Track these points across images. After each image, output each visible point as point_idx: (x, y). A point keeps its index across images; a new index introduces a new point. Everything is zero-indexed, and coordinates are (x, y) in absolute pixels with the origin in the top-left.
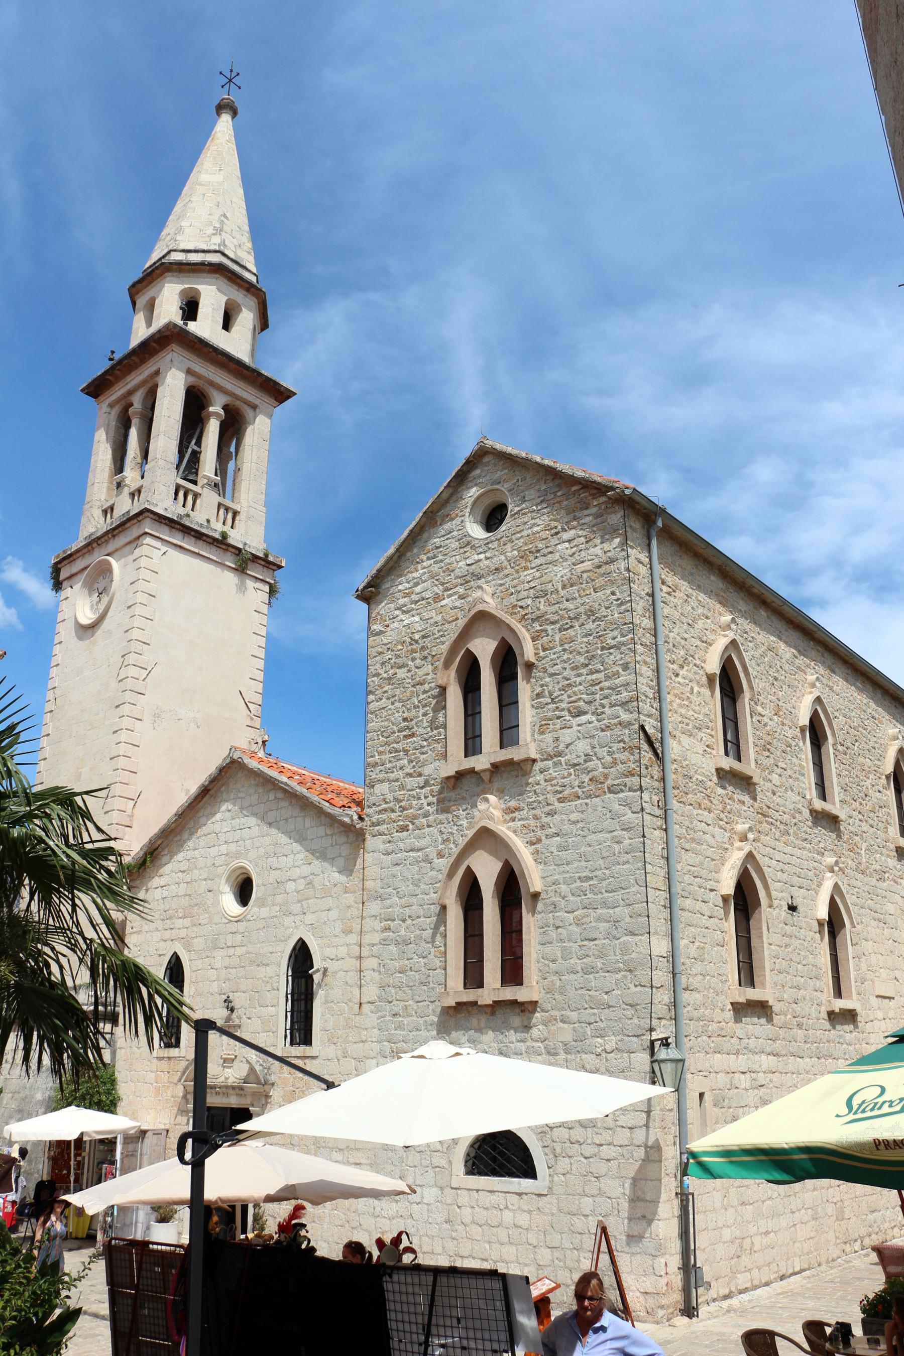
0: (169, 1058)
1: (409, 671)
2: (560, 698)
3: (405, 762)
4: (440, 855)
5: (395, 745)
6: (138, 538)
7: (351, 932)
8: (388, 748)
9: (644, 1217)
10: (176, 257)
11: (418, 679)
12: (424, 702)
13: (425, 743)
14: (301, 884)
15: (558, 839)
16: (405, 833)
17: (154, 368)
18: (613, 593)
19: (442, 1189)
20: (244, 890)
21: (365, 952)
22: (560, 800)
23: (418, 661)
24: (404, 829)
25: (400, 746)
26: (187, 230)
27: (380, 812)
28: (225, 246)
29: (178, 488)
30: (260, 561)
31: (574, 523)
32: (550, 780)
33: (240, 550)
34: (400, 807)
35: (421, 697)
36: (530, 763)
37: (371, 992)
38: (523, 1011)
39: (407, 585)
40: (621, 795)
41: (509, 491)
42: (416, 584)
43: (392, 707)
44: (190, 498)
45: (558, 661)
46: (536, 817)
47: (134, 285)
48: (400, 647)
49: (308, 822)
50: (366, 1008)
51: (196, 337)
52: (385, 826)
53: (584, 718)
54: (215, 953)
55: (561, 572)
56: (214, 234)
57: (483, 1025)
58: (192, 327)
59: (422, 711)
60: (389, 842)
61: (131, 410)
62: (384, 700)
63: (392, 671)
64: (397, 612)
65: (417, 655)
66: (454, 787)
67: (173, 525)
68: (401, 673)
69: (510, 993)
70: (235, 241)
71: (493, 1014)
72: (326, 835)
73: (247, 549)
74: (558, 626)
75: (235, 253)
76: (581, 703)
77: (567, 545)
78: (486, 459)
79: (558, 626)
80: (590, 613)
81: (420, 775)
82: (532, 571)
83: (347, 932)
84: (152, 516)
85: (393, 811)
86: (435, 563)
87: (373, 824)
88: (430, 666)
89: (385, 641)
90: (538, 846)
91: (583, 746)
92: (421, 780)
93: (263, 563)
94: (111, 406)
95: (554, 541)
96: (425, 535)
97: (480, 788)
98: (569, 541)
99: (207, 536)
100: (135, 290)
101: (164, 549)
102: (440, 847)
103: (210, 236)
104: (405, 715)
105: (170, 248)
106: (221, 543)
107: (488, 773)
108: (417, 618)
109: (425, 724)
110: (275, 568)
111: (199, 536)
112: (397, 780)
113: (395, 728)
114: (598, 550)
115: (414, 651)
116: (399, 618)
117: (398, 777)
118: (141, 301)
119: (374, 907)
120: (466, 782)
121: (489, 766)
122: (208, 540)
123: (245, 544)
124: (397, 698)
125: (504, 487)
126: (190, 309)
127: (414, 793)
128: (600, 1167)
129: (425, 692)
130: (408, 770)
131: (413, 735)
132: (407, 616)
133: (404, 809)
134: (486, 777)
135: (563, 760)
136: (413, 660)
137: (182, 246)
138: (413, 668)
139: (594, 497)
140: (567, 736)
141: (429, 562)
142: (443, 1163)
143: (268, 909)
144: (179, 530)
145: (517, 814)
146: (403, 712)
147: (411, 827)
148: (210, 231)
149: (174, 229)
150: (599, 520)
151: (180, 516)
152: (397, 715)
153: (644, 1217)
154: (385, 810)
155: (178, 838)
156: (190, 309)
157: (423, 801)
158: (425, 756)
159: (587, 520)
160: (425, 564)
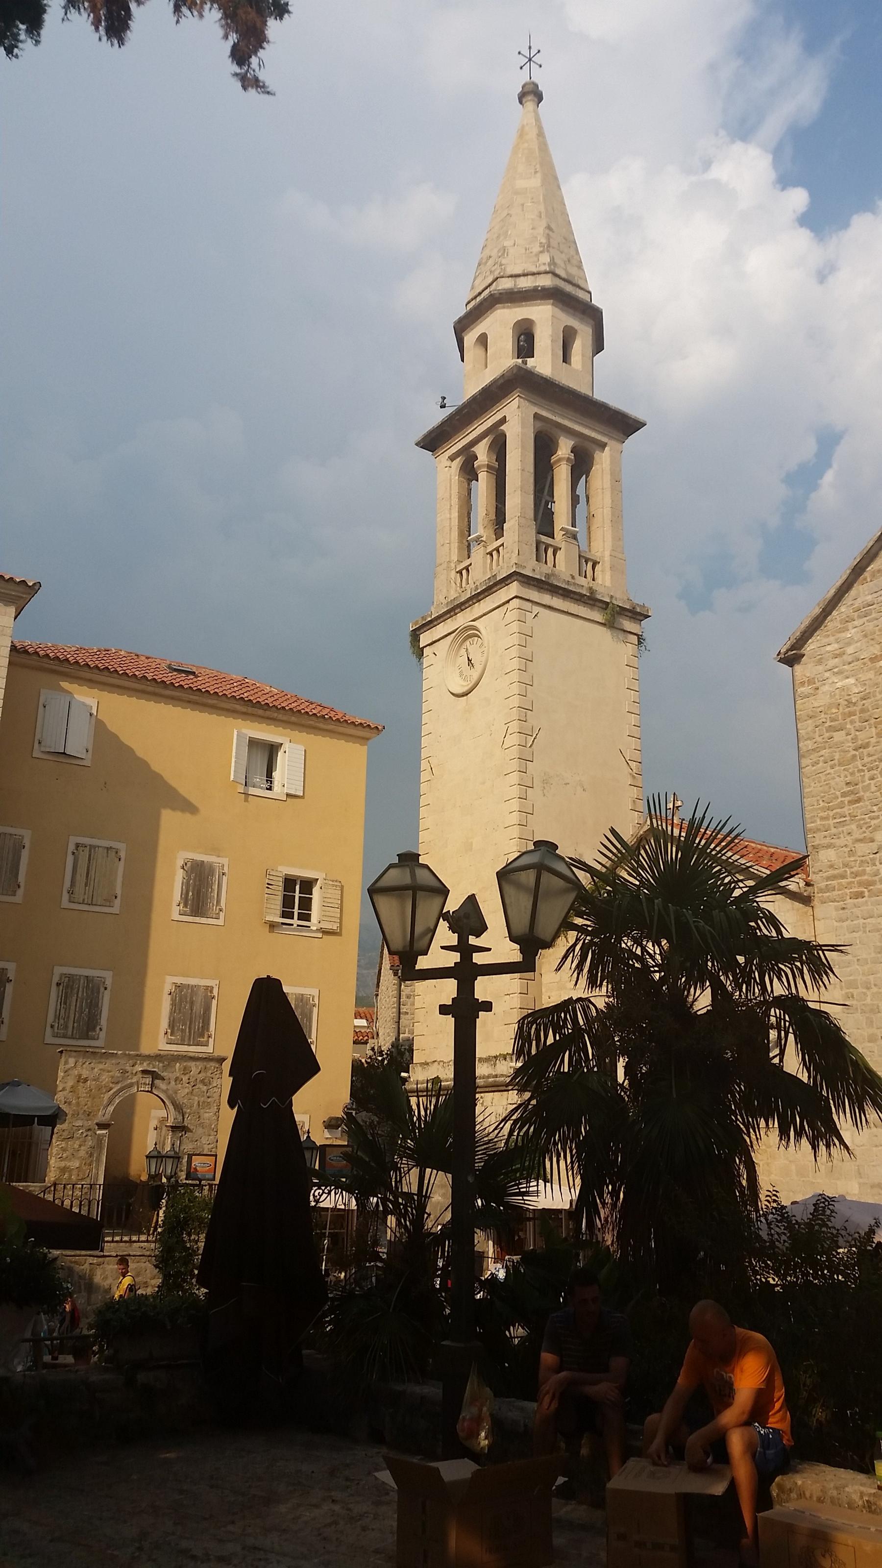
1: (848, 734)
3: (854, 827)
5: (838, 810)
6: (508, 602)
8: (831, 813)
10: (506, 284)
11: (860, 742)
12: (868, 765)
13: (875, 808)
16: (860, 900)
17: (498, 417)
23: (858, 724)
24: (861, 895)
25: (846, 810)
26: (512, 251)
27: (828, 879)
28: (555, 264)
29: (538, 543)
30: (627, 613)
33: (607, 604)
34: (852, 873)
35: (866, 760)
39: (836, 646)
42: (849, 644)
43: (832, 771)
44: (550, 551)
47: (460, 321)
48: (834, 711)
51: (542, 378)
52: (836, 893)
56: (541, 252)
58: (531, 362)
59: (868, 775)
60: (844, 908)
61: (476, 464)
62: (821, 764)
63: (827, 735)
64: (827, 674)
65: (856, 718)
67: (541, 585)
68: (839, 736)
70: (563, 256)
73: (615, 602)
75: (566, 270)
81: (873, 841)
84: (520, 578)
85: (843, 877)
86: (868, 621)
87: (821, 891)
88: (873, 729)
89: (816, 705)
92: (874, 846)
93: (630, 614)
94: (452, 458)
99: (574, 593)
100: (461, 327)
101: (536, 609)
103: (537, 255)
104: (848, 779)
105: (496, 274)
106: (590, 600)
108: (852, 681)
109: (873, 789)
110: (641, 618)
111: (566, 594)
113: (838, 793)
115: (851, 714)
116: (830, 681)
117: (846, 842)
118: (470, 338)
122: (575, 597)
123: (612, 597)
124: (836, 761)
126: (525, 342)
127: (867, 858)
129: (869, 755)
130: (857, 835)
131: (859, 800)
132: (840, 677)
133: (856, 875)
136: (852, 722)
137: (510, 270)
138: (853, 732)
141: (861, 621)
144: (547, 590)
147: (866, 894)
148: (536, 248)
149: (496, 250)
151: (547, 576)
152: (838, 779)
154: (834, 877)
156: (525, 342)
158: (876, 822)
160: (856, 623)
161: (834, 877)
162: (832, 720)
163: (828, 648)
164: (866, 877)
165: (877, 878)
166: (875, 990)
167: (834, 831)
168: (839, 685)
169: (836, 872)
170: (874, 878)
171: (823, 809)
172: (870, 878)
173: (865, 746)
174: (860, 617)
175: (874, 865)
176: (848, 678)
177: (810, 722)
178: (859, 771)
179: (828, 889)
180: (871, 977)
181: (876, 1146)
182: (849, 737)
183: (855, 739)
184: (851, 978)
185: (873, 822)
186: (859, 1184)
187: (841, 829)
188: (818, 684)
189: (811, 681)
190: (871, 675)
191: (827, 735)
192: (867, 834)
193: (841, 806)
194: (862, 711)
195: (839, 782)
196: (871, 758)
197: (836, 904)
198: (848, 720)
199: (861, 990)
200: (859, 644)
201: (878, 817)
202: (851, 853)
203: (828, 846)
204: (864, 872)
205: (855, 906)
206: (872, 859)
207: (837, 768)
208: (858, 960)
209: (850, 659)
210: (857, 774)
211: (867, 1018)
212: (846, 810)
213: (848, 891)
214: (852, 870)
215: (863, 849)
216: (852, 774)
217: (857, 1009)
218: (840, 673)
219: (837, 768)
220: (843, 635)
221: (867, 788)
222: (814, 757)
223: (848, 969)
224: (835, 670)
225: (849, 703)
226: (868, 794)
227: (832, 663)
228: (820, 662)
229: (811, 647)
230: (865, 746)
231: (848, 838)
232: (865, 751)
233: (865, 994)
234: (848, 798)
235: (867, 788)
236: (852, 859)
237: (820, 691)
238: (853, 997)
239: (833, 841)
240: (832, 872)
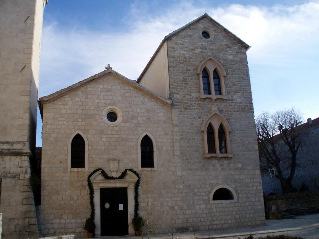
0: (78, 171)
1: (185, 66)
2: (232, 87)
4: (199, 118)
5: (181, 85)
7: (168, 135)
8: (178, 85)
9: (261, 205)
11: (188, 69)
13: (192, 87)
14: (145, 119)
15: (234, 120)
16: (186, 110)
18: (244, 67)
19: (206, 204)
20: (112, 116)
21: (175, 141)
22: (234, 111)
23: (187, 64)
24: (187, 109)
25: (183, 85)
27: (176, 102)
31: (233, 47)
32: (231, 106)
34: (184, 102)
35: (190, 74)
36: (226, 100)
37: (178, 153)
38: (228, 160)
40: (249, 113)
41: (213, 31)
45: (231, 78)
46: (227, 114)
48: (180, 58)
49: (146, 100)
50: (176, 157)
52: (179, 107)
53: (239, 94)
54: (102, 136)
55: (231, 57)
57: (216, 163)
59: (190, 78)
60: (181, 111)
62: (175, 71)
66: (203, 101)
68: (182, 65)
69: (225, 155)
71: (219, 160)
72: (154, 105)
74: (231, 70)
76: (238, 90)
77: (231, 51)
78: (205, 19)
79: (231, 70)
80: (239, 70)
81: (191, 95)
82: (222, 54)
83: (166, 135)
89: (175, 55)
90: (229, 121)
91: (239, 100)
92: (191, 97)
95: (228, 49)
96: (187, 30)
97: (211, 103)
98: (232, 51)
102: (199, 116)
104: (184, 77)
107: (215, 100)
108: (185, 52)
112: (183, 95)
114: (240, 56)
119: (176, 129)
120: (207, 101)
121: (216, 99)
125: (212, 29)
128: (250, 195)
129: (191, 73)
130: (186, 92)
131: (187, 84)
133: (186, 103)
134: (214, 101)
135: (234, 102)
139: (238, 43)
140: (235, 97)
142: (207, 198)
143: (129, 124)
145: (222, 112)
146: (183, 76)
150: (239, 49)
153: (261, 205)
154: (178, 102)
155: (75, 92)
157: (193, 103)
158: (192, 91)
159: (236, 48)
161: (178, 102)
162: (180, 61)
163: (179, 41)
164: (188, 104)
165: (192, 105)
166: (190, 134)
167: (179, 90)
168: (182, 52)
169: (179, 101)
170: (191, 105)
171: (176, 83)
172: (190, 105)
173: (190, 70)
174: (188, 37)
175: (191, 102)
176: (184, 51)
177: (172, 58)
178: (188, 76)
179: (176, 105)
180: (189, 131)
181: (189, 175)
182: (185, 67)
183: (187, 68)
184: (182, 130)
185: (191, 91)
186: (183, 186)
187: (181, 90)
188: (175, 50)
189: (173, 48)
190: (191, 53)
191: (178, 64)
192: (189, 93)
193: (182, 83)
194: (189, 61)
195: (181, 77)
196: (191, 74)
197: (178, 110)
198: (185, 62)
199: (186, 134)
200: (188, 44)
201: (193, 90)
202: (184, 97)
203: (177, 94)
204: (188, 103)
205: (185, 111)
206: (191, 100)
207: (181, 73)
208: (185, 126)
209: (185, 47)
210: (187, 77)
211: (187, 141)
212: (183, 85)
213: (183, 107)
214: (184, 102)
215: (188, 97)
216: (185, 76)
217: (184, 139)
218: (182, 49)
219: (181, 73)
220: (184, 40)
221: (190, 81)
222: (173, 68)
223: (182, 128)
224: (181, 48)
225: (185, 58)
226: (190, 83)
227: (180, 46)
228: (176, 44)
229: (174, 39)
230: (190, 70)
231: (183, 93)
232: (190, 72)
233: (187, 135)
234: (184, 83)
235: (190, 81)
236: (184, 99)
237: (176, 52)
238: (183, 135)
239: (179, 93)
240: (177, 101)
